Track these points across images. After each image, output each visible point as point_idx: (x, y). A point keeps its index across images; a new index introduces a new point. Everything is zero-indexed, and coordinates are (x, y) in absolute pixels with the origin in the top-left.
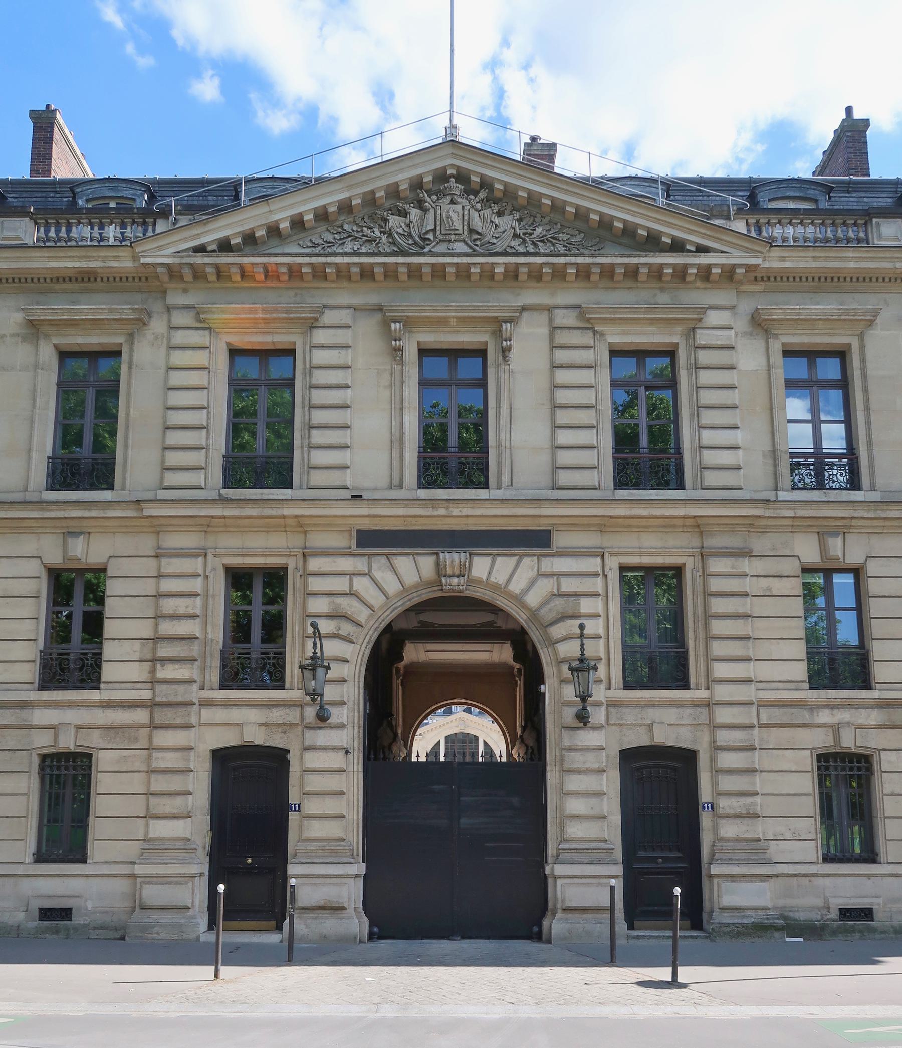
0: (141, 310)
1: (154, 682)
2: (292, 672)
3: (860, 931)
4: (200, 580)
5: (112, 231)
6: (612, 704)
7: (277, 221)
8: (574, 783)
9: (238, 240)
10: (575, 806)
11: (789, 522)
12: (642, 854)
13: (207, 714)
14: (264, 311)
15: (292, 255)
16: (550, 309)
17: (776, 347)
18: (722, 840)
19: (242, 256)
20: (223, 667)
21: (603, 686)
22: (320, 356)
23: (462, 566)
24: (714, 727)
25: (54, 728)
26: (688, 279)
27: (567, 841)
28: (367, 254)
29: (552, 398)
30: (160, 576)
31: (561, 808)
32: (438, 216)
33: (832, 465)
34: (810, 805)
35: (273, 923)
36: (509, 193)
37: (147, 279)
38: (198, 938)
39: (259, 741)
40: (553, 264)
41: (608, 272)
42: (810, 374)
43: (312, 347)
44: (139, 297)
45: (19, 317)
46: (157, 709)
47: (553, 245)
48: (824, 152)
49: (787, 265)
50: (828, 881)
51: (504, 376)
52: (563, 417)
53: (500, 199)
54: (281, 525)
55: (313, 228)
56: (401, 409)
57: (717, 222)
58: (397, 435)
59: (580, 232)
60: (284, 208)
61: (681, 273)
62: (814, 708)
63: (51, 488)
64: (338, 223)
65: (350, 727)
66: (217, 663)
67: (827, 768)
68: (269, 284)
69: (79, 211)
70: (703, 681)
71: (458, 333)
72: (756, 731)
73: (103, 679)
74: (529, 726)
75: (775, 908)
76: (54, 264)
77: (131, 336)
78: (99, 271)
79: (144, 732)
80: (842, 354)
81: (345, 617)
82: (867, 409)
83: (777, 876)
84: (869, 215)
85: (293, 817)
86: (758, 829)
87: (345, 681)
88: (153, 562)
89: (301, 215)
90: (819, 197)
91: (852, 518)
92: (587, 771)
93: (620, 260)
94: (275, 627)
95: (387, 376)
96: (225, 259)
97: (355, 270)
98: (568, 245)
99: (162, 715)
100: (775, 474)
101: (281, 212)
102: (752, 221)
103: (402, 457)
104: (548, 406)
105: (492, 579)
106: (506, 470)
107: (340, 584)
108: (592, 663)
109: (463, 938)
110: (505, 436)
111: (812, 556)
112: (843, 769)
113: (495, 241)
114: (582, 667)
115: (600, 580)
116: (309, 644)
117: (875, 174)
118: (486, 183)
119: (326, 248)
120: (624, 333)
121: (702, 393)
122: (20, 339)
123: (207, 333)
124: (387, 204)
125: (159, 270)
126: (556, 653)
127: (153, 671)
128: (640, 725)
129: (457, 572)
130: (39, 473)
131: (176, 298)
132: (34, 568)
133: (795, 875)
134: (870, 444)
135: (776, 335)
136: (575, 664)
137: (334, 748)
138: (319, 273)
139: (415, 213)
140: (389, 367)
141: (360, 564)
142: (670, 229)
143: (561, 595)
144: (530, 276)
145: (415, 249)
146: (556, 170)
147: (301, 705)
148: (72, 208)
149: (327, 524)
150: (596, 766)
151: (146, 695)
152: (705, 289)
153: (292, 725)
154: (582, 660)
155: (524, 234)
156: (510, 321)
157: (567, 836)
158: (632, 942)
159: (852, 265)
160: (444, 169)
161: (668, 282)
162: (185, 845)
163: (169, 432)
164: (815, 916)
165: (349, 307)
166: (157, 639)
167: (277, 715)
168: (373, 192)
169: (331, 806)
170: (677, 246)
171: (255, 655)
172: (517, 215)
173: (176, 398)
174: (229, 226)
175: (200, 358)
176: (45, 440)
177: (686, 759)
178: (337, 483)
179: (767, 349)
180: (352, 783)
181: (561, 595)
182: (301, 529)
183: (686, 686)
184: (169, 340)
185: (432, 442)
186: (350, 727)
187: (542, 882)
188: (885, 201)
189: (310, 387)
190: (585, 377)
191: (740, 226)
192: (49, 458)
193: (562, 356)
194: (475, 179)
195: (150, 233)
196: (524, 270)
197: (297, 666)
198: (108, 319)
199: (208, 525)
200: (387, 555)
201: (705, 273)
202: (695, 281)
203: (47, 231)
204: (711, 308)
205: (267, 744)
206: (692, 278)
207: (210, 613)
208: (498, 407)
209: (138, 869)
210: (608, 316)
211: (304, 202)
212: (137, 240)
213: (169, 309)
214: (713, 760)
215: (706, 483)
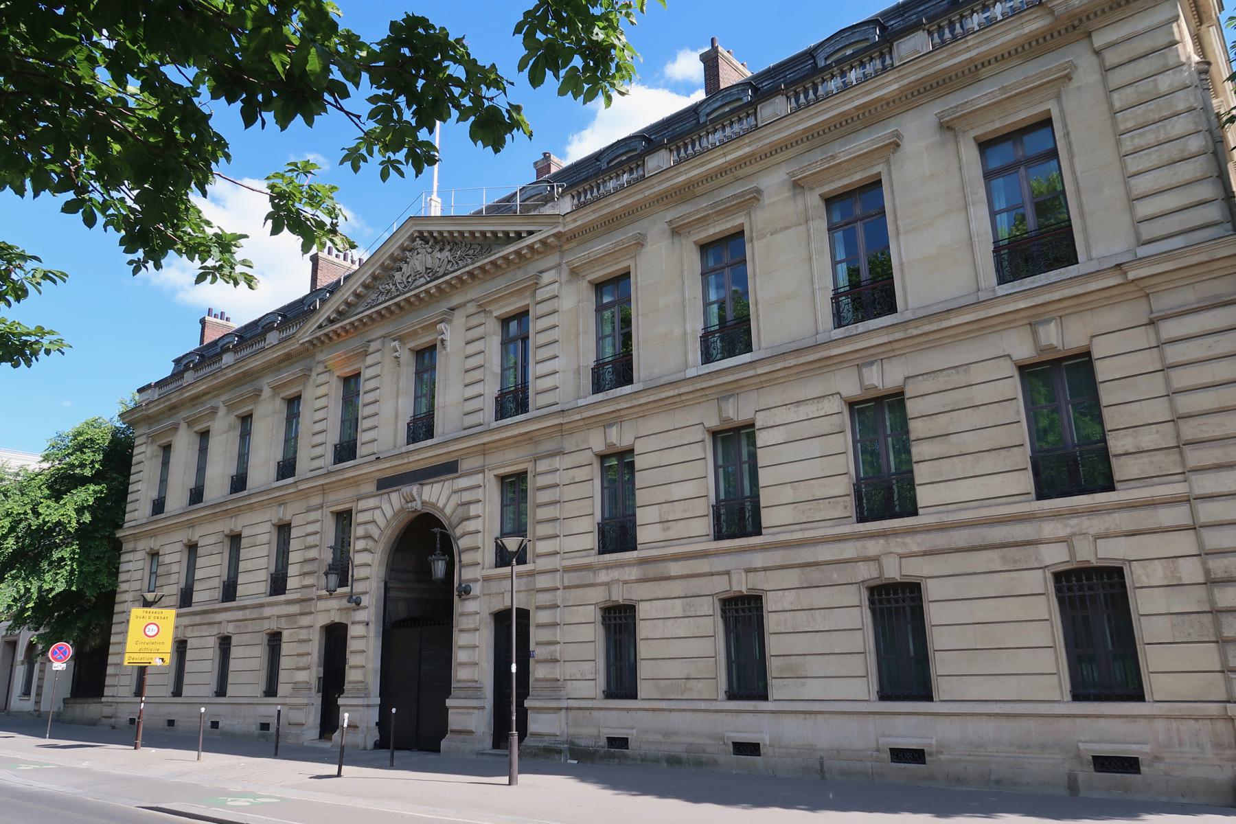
11: (581, 423)
120: (502, 307)
133: (580, 709)
139: (405, 267)
170: (519, 236)
204: (541, 272)
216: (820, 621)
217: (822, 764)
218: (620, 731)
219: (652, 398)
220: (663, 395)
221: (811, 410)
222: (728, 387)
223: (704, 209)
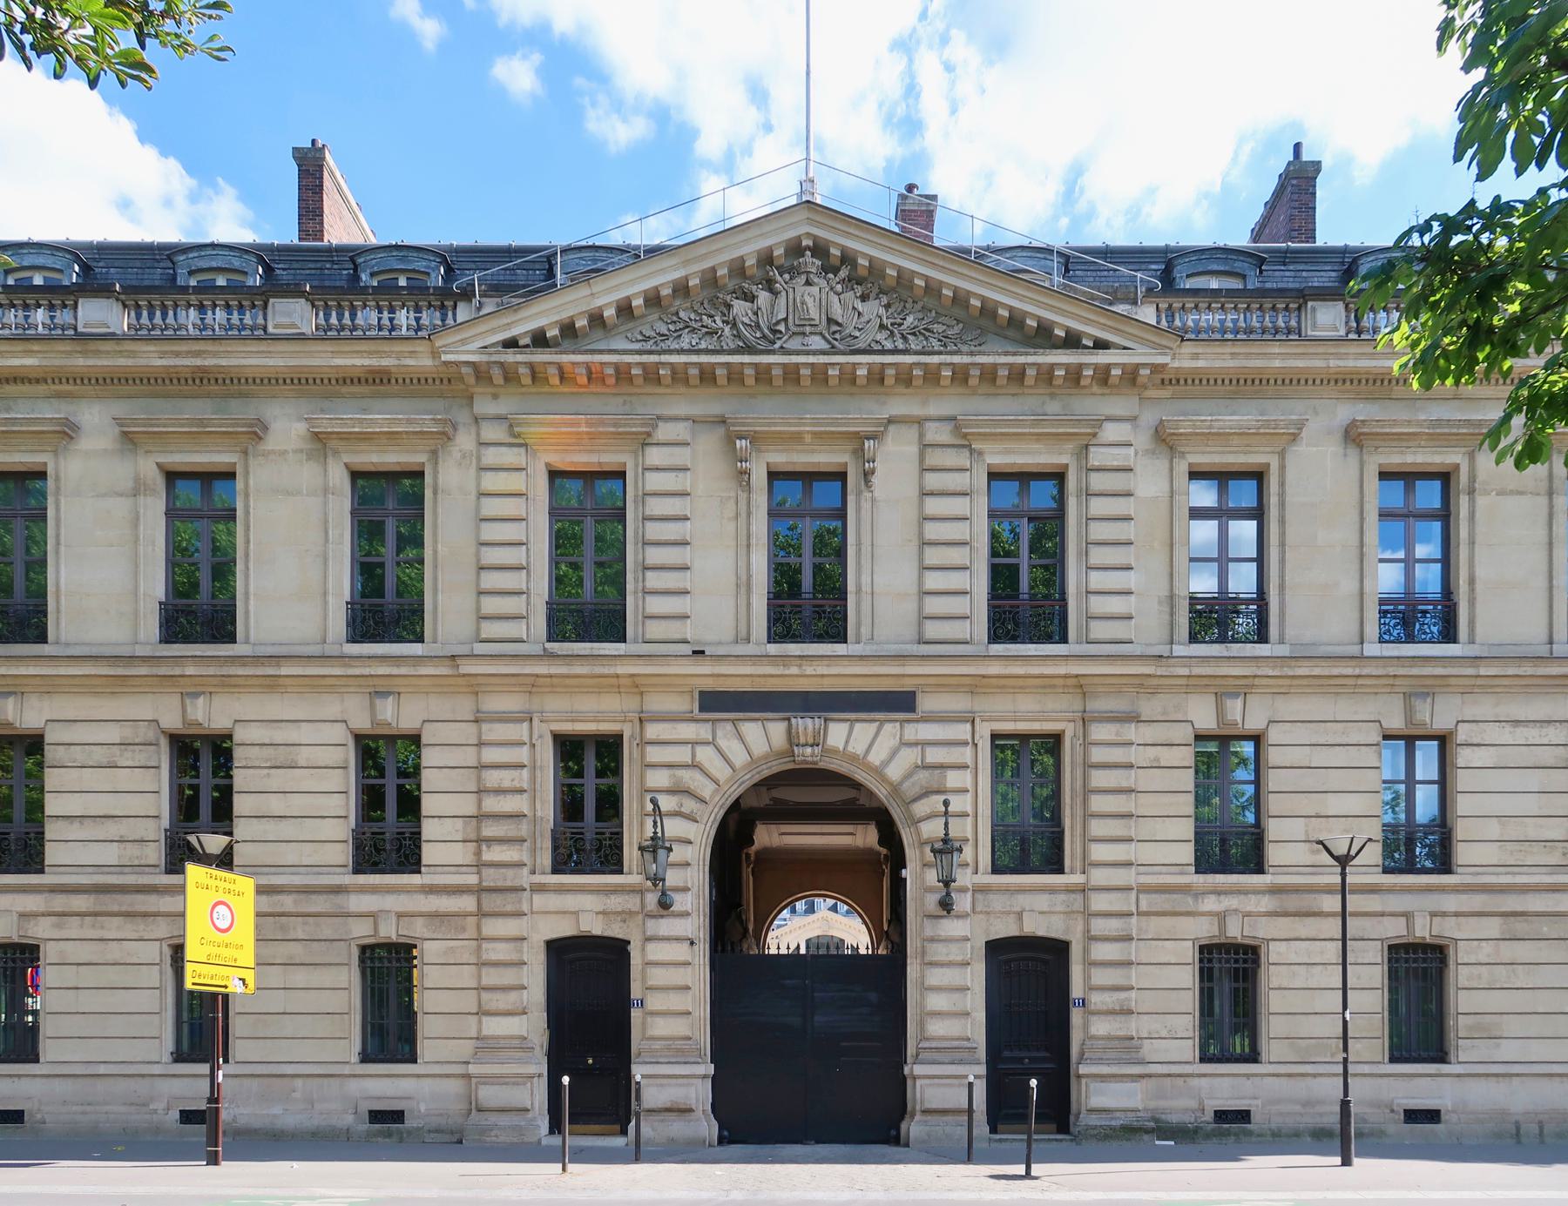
0: (444, 422)
1: (480, 865)
2: (630, 854)
3: (1236, 1135)
4: (526, 749)
6: (979, 890)
7: (600, 308)
8: (936, 977)
10: (936, 1002)
12: (1007, 1054)
13: (539, 901)
14: (588, 424)
15: (620, 351)
16: (920, 422)
17: (1182, 468)
18: (1093, 1038)
20: (555, 848)
21: (969, 871)
22: (655, 481)
23: (816, 734)
24: (1088, 915)
25: (373, 916)
26: (1083, 383)
27: (927, 1039)
28: (707, 352)
29: (921, 534)
30: (481, 744)
31: (922, 1005)
34: (1189, 1001)
35: (618, 1127)
36: (876, 269)
38: (539, 1141)
39: (597, 931)
43: (645, 469)
44: (440, 404)
45: (300, 428)
46: (484, 895)
49: (1201, 364)
50: (1204, 1080)
51: (866, 506)
52: (933, 556)
53: (861, 278)
54: (615, 685)
55: (643, 316)
56: (748, 546)
58: (744, 578)
59: (958, 322)
60: (609, 291)
61: (1074, 375)
62: (1198, 894)
63: (352, 639)
64: (673, 310)
65: (694, 915)
66: (548, 844)
67: (1210, 961)
68: (593, 388)
70: (1078, 865)
71: (813, 451)
72: (1134, 919)
73: (424, 862)
74: (890, 921)
75: (1146, 1110)
77: (434, 453)
79: (472, 920)
80: (1258, 476)
81: (687, 792)
82: (1282, 544)
83: (1150, 1076)
84: (1303, 297)
85: (635, 1014)
86: (1132, 1026)
87: (688, 864)
88: (472, 728)
89: (628, 300)
90: (1247, 272)
92: (950, 964)
94: (610, 804)
95: (731, 505)
96: (540, 357)
97: (694, 372)
98: (944, 339)
99: (492, 902)
100: (1172, 624)
101: (604, 295)
102: (1163, 306)
103: (749, 604)
104: (916, 542)
105: (850, 748)
106: (866, 621)
107: (681, 754)
108: (957, 845)
109: (818, 1142)
110: (866, 579)
111: (1206, 720)
112: (1228, 961)
114: (946, 848)
115: (969, 750)
116: (649, 822)
117: (1319, 243)
118: (848, 258)
120: (1008, 452)
123: (523, 450)
124: (730, 286)
125: (464, 370)
126: (918, 834)
127: (478, 853)
128: (1008, 913)
129: (811, 741)
130: (338, 623)
131: (484, 406)
132: (339, 734)
134: (1282, 587)
136: (938, 845)
137: (678, 939)
138: (651, 375)
139: (763, 297)
140: (733, 494)
141: (703, 731)
142: (1064, 320)
143: (926, 767)
144: (897, 379)
145: (763, 345)
147: (641, 892)
148: (354, 286)
149: (666, 684)
150: (959, 958)
151: (472, 879)
153: (631, 913)
154: (946, 840)
157: (927, 1034)
158: (994, 1145)
159: (1277, 363)
162: (522, 1044)
163: (483, 574)
164: (1188, 1118)
165: (686, 419)
166: (480, 817)
167: (615, 902)
168: (713, 269)
169: (676, 1002)
171: (589, 836)
173: (492, 532)
174: (544, 314)
175: (515, 482)
176: (341, 583)
177: (1059, 949)
178: (677, 636)
179: (1171, 470)
180: (697, 976)
181: (926, 767)
183: (1061, 871)
184: (479, 459)
185: (784, 582)
186: (694, 915)
187: (899, 1084)
188: (1325, 277)
190: (958, 506)
191: (1147, 314)
193: (933, 481)
195: (450, 321)
197: (636, 847)
199: (533, 685)
200: (733, 721)
201: (1103, 375)
203: (327, 317)
204: (1109, 419)
205: (606, 934)
207: (538, 786)
208: (859, 544)
209: (472, 1069)
211: (633, 282)
212: (434, 331)
214: (1086, 951)
215: (1092, 636)
216: (1522, 977)
217: (1518, 1129)
218: (1238, 1102)
219: (1317, 672)
220: (1335, 671)
221: (1532, 735)
222: (1428, 682)
223: (1419, 423)
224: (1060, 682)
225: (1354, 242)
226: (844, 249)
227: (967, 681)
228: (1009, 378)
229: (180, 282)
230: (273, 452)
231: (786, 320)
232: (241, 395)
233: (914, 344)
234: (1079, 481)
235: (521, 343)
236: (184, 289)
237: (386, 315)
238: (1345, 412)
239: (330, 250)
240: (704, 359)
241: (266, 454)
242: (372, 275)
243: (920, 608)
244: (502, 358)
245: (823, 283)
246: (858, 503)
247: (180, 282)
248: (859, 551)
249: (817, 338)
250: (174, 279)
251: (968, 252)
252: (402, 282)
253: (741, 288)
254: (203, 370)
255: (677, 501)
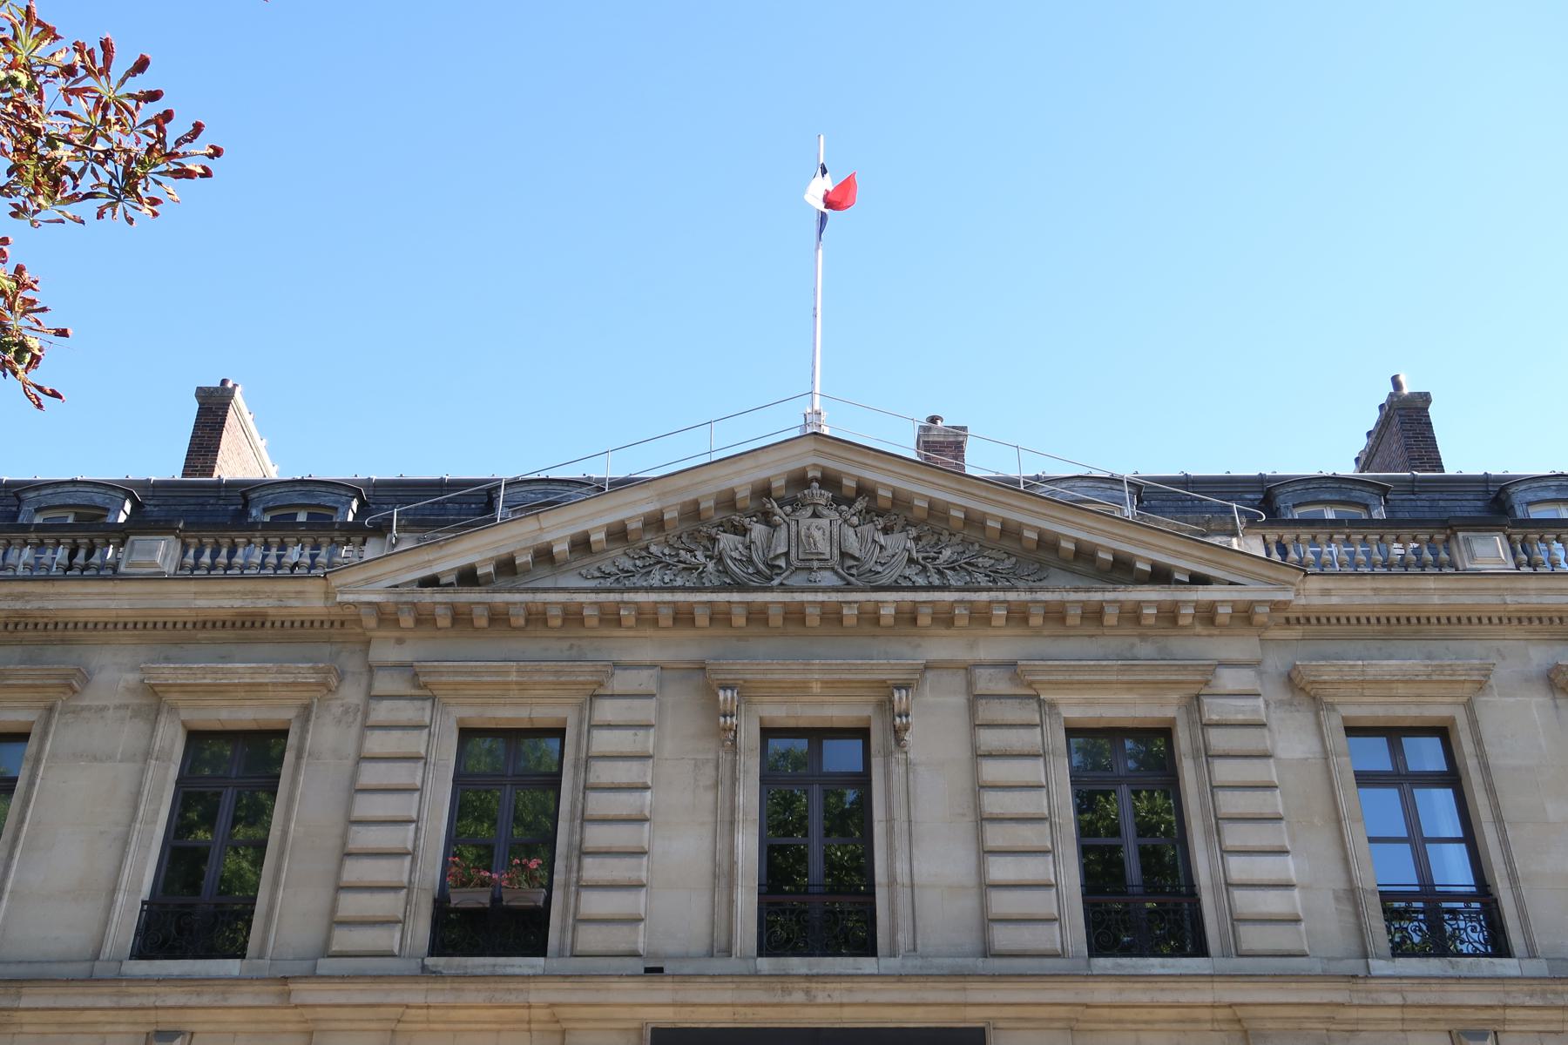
5: (293, 554)
9: (491, 569)
16: (969, 668)
17: (1334, 723)
19: (494, 592)
22: (604, 741)
28: (684, 589)
32: (793, 534)
33: (1452, 911)
36: (901, 502)
37: (342, 624)
40: (971, 602)
41: (1056, 615)
42: (1395, 764)
43: (591, 727)
44: (326, 649)
45: (132, 678)
47: (969, 574)
48: (1369, 434)
49: (1335, 600)
51: (898, 771)
55: (604, 551)
56: (732, 823)
57: (1217, 540)
58: (725, 866)
59: (1009, 555)
61: (1169, 615)
63: (140, 953)
69: (253, 527)
71: (822, 703)
76: (202, 603)
77: (306, 712)
78: (271, 611)
82: (1499, 820)
84: (1451, 526)
91: (1505, 1007)
93: (1073, 596)
95: (709, 771)
100: (1361, 930)
101: (557, 528)
103: (731, 902)
106: (904, 923)
110: (901, 867)
113: (880, 569)
117: (1450, 469)
118: (864, 490)
119: (622, 580)
120: (1090, 703)
121: (1222, 796)
122: (129, 713)
124: (717, 519)
125: (363, 610)
131: (386, 651)
134: (1513, 878)
135: (1332, 704)
138: (611, 618)
139: (758, 531)
140: (711, 756)
142: (1147, 551)
146: (968, 471)
152: (1210, 636)
155: (925, 558)
156: (906, 686)
159: (1436, 600)
160: (804, 471)
161: (1150, 627)
165: (652, 666)
168: (696, 503)
170: (1160, 575)
172: (913, 532)
173: (368, 807)
175: (415, 743)
176: (142, 874)
178: (623, 947)
182: (557, 1026)
184: (366, 715)
189: (585, 788)
190: (1030, 771)
192: (144, 903)
193: (990, 739)
194: (849, 483)
196: (927, 610)
198: (274, 684)
201: (1208, 614)
202: (1192, 626)
206: (1188, 621)
208: (890, 820)
210: (1060, 678)
213: (371, 669)
224: (1206, 1014)
225: (1495, 471)
226: (859, 481)
227: (1062, 1012)
228: (1083, 617)
229: (22, 519)
230: (89, 708)
231: (787, 554)
232: (63, 642)
233: (953, 579)
234: (1193, 739)
235: (443, 581)
236: (25, 528)
237: (274, 551)
238: (1540, 655)
239: (219, 484)
240: (680, 597)
241: (76, 711)
242: (265, 510)
243: (984, 907)
244: (416, 598)
245: (834, 515)
246: (887, 766)
247: (22, 519)
248: (890, 832)
249: (828, 574)
250: (16, 516)
251: (1017, 482)
252: (302, 517)
253: (731, 521)
254: (23, 614)
255: (635, 766)
